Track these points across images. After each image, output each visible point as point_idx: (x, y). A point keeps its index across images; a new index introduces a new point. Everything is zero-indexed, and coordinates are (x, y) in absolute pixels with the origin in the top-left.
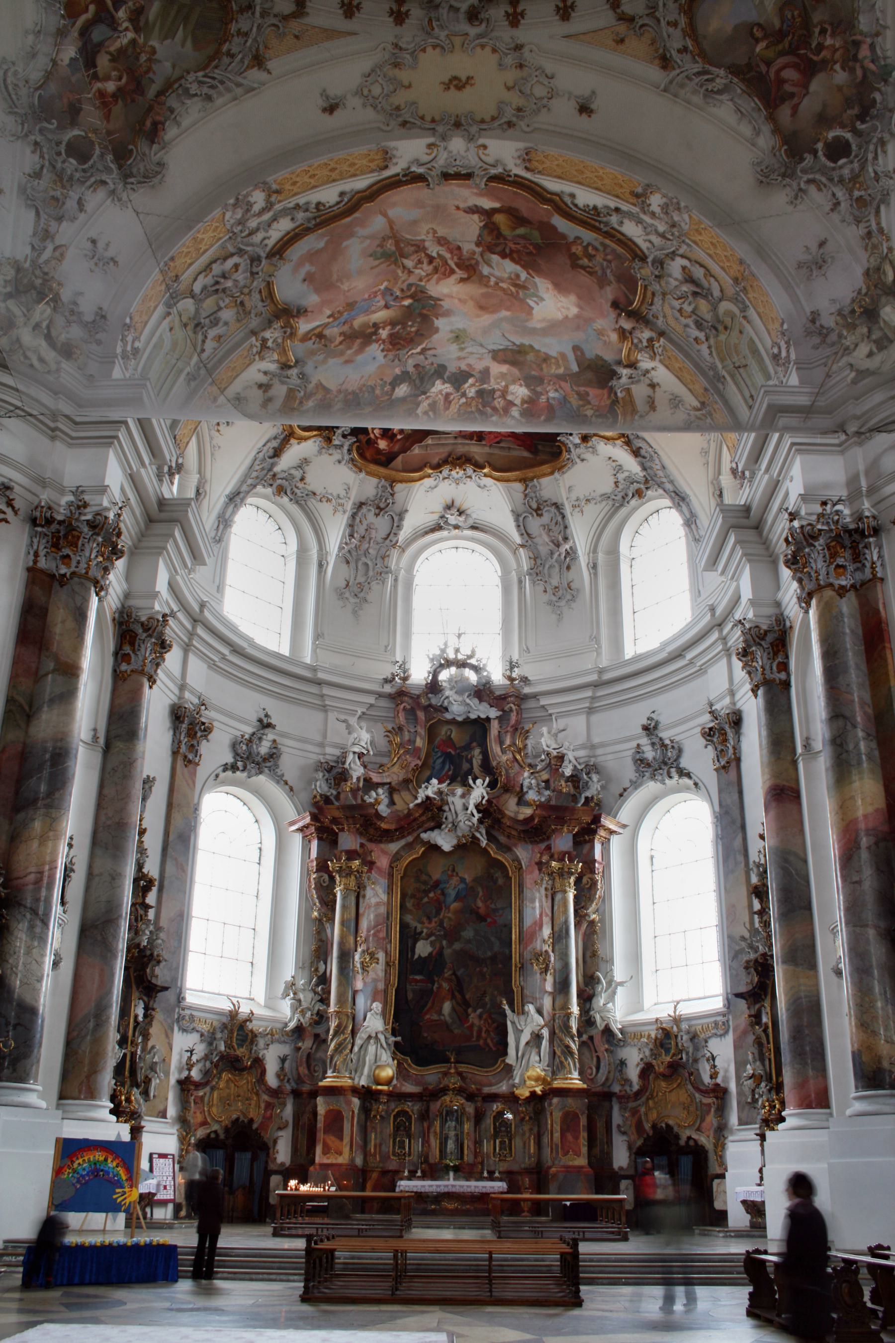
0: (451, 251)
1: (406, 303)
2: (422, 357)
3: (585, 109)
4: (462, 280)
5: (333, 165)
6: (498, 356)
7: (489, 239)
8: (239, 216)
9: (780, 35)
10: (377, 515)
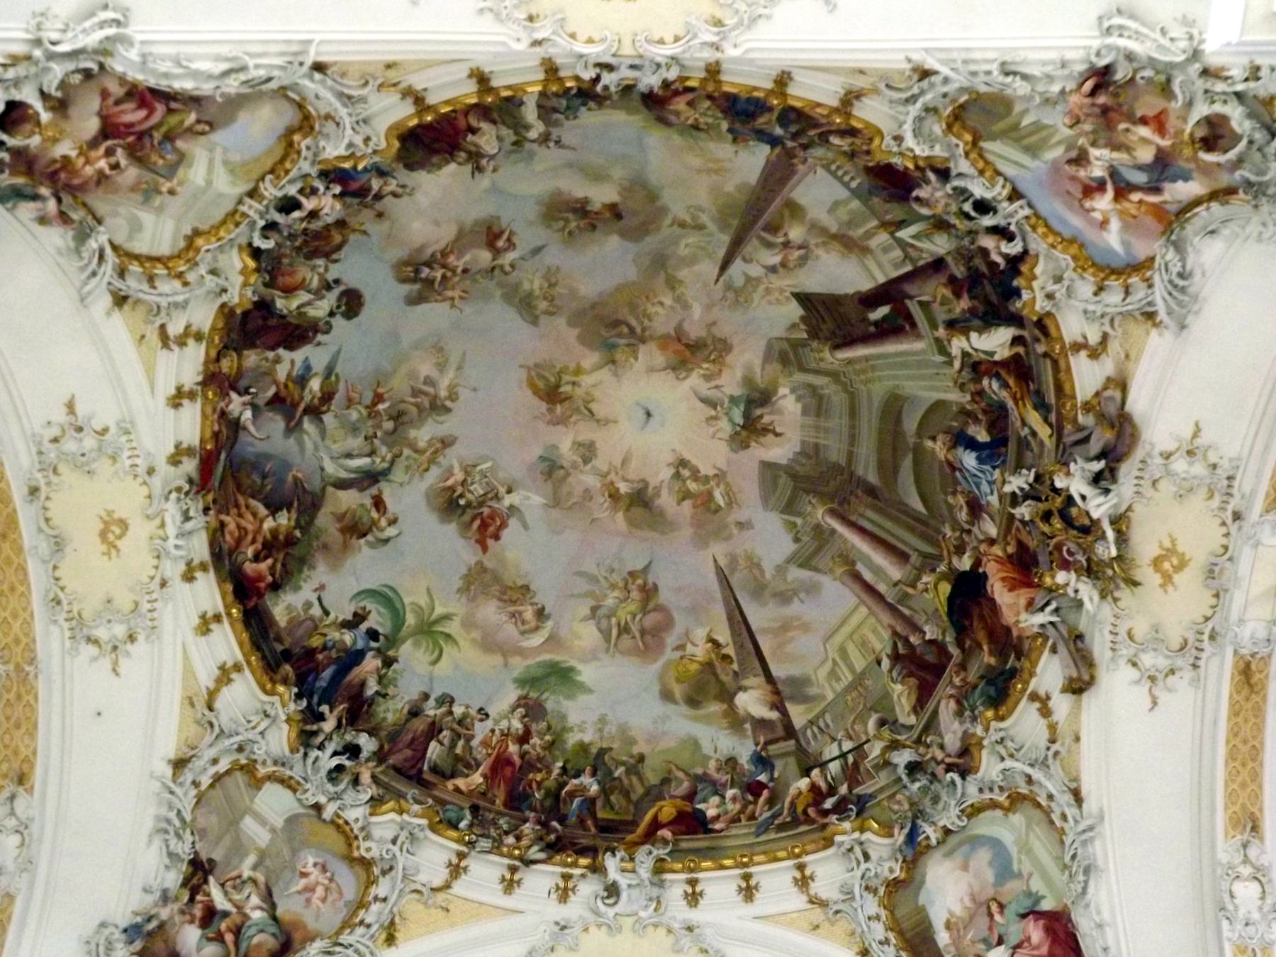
9: (169, 138)
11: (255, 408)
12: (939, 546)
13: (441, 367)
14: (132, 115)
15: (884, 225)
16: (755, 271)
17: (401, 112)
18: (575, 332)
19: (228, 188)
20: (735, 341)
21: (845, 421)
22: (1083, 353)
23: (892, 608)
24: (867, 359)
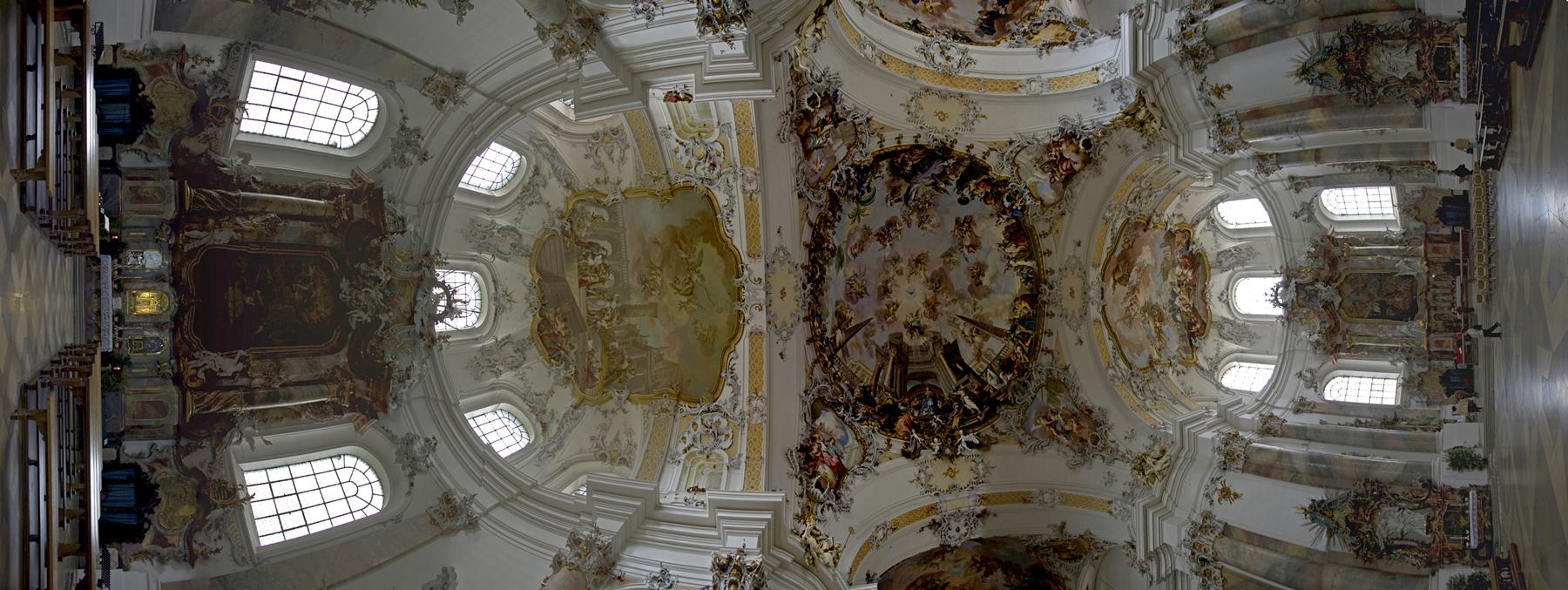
6: (1165, 278)
12: (901, 396)
23: (876, 384)
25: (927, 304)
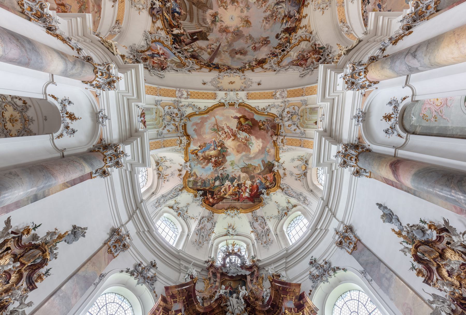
0: (230, 130)
1: (219, 148)
2: (223, 171)
3: (259, 84)
4: (233, 140)
5: (203, 94)
7: (239, 126)
8: (180, 95)
9: (298, 59)
10: (208, 222)
11: (295, 16)
13: (265, 26)
14: (303, 62)
15: (195, 51)
16: (215, 44)
17: (266, 66)
18: (243, 33)
19: (292, 53)
20: (218, 32)
21: (199, 17)
22: (161, 28)
24: (197, 29)
25: (227, 28)
